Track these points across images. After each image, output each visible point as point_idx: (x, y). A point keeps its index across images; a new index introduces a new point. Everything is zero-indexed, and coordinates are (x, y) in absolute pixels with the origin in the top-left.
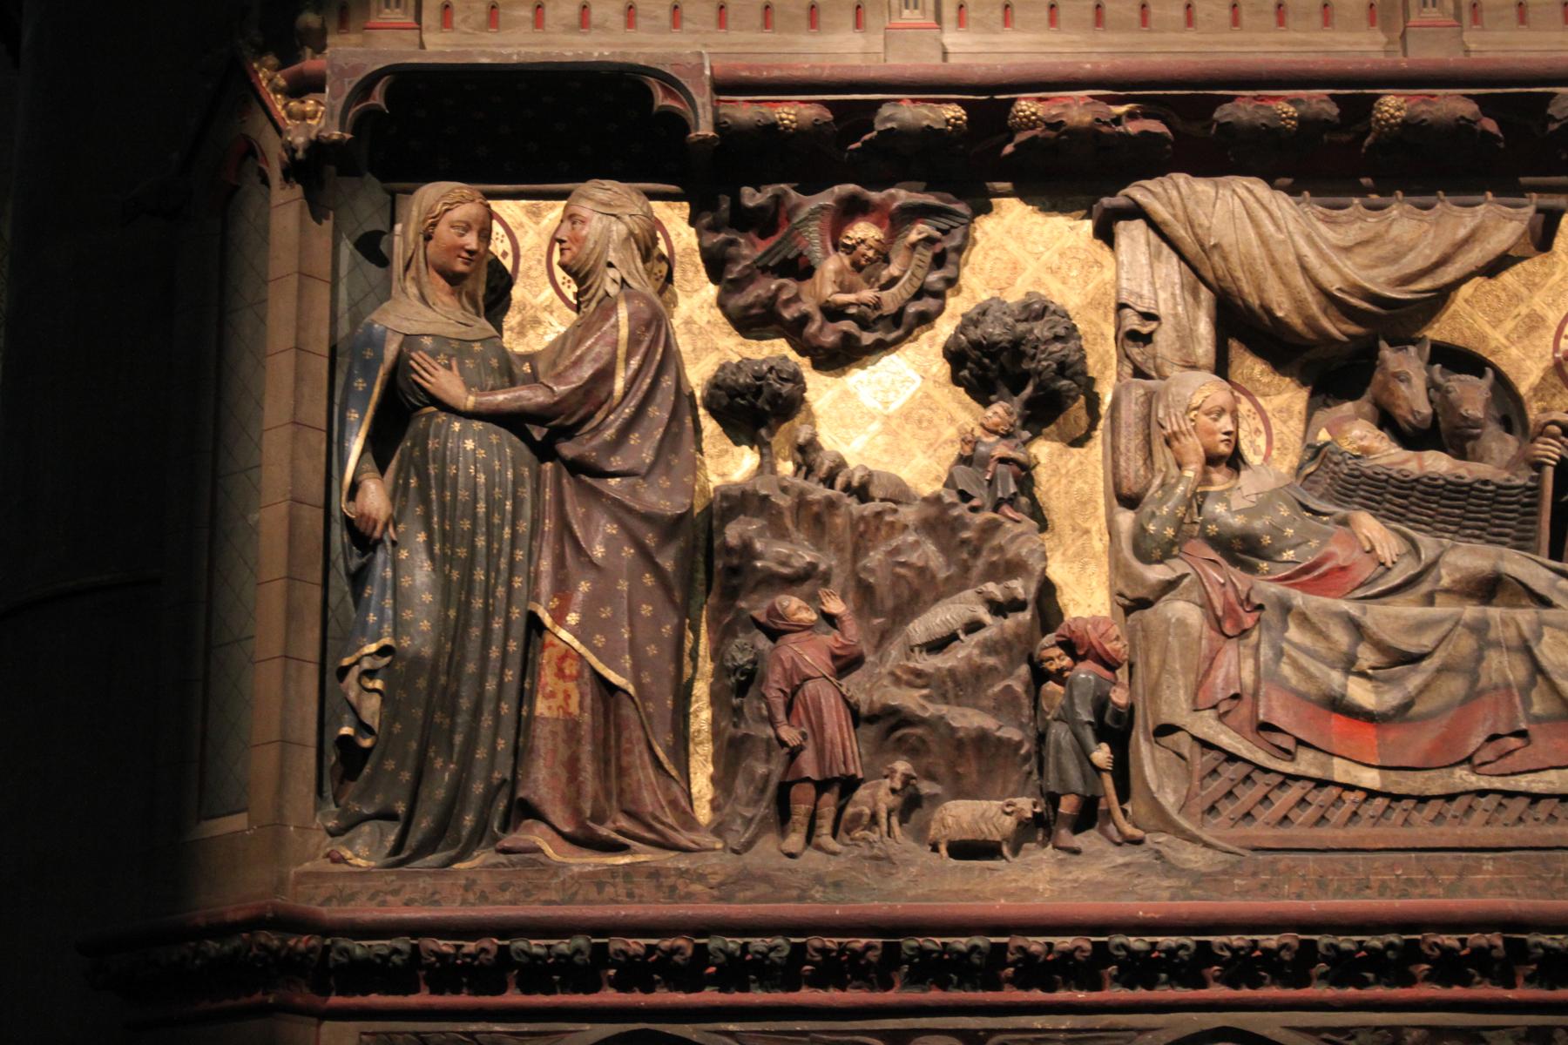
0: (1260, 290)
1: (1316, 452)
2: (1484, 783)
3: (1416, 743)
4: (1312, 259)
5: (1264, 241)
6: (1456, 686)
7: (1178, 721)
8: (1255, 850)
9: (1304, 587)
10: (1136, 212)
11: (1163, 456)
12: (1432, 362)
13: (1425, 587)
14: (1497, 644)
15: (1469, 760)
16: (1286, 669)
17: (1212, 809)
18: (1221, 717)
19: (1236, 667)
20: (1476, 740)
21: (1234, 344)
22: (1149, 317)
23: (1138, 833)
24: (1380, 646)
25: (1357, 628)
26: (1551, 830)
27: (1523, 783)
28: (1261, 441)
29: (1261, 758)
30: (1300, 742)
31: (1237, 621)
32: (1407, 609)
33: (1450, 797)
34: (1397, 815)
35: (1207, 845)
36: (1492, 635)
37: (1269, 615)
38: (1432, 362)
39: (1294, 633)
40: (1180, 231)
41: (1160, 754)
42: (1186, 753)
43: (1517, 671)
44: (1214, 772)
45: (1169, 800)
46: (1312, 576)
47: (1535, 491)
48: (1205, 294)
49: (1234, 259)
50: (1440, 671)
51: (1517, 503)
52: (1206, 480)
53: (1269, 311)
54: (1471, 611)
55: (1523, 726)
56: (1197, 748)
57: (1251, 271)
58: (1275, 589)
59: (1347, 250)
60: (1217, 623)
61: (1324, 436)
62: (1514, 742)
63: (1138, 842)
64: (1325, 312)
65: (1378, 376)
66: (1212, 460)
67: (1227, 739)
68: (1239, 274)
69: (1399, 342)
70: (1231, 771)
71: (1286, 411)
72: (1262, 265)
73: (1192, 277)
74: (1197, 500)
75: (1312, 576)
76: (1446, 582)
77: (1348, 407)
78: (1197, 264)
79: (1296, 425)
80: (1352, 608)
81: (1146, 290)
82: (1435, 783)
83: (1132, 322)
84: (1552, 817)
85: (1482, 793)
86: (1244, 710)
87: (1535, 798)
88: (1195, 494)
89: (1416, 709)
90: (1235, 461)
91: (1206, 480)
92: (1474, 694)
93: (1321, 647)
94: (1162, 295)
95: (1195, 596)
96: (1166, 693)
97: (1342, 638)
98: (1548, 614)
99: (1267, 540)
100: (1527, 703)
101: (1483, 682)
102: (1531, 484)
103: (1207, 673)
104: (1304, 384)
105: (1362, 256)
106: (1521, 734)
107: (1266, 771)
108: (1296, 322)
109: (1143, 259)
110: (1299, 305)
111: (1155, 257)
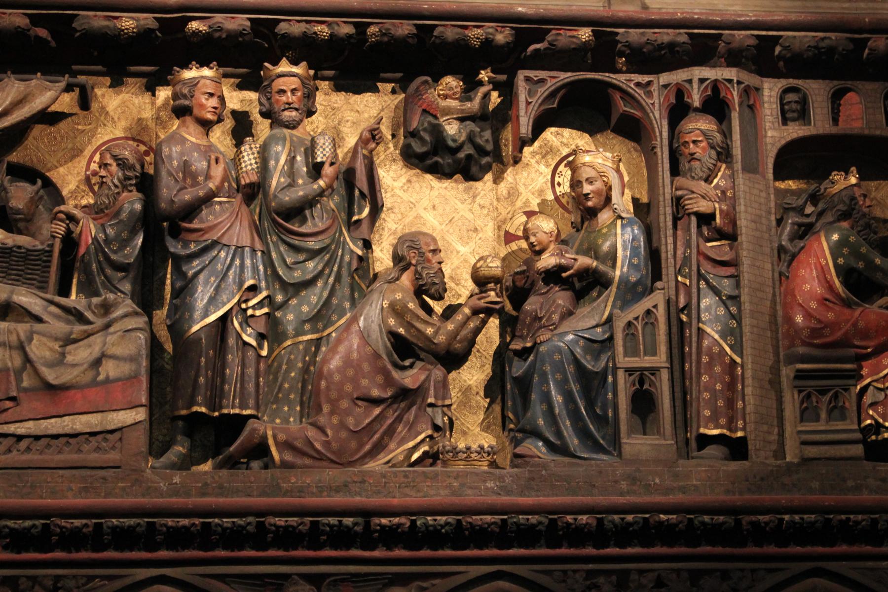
51: (40, 260)
98: (38, 327)
102: (47, 249)
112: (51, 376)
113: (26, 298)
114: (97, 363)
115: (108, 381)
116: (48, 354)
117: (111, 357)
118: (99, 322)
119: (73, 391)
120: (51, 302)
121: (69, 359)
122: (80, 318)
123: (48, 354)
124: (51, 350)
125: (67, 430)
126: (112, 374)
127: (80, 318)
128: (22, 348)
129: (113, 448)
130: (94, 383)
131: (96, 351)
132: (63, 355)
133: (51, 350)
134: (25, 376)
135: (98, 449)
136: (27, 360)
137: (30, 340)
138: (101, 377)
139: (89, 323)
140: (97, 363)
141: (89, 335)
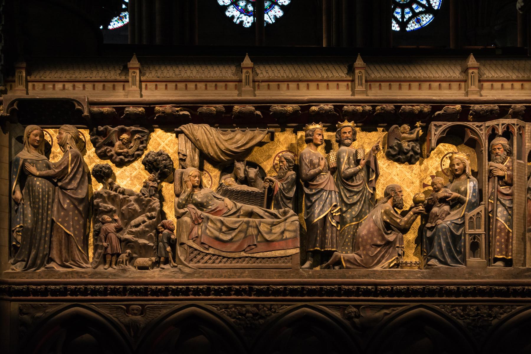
0: (207, 150)
1: (221, 185)
2: (247, 255)
3: (234, 247)
4: (218, 143)
5: (208, 139)
6: (242, 235)
7: (184, 242)
8: (200, 268)
9: (212, 214)
10: (182, 132)
11: (184, 186)
12: (246, 165)
13: (238, 214)
14: (251, 226)
15: (244, 250)
16: (207, 231)
17: (191, 260)
18: (194, 241)
19: (197, 231)
20: (245, 246)
21: (205, 161)
22: (184, 155)
23: (176, 265)
24: (227, 227)
25: (222, 222)
26: (260, 264)
27: (255, 255)
28: (210, 182)
29: (202, 250)
30: (210, 247)
31: (198, 221)
32: (233, 219)
33: (240, 258)
34: (229, 262)
35: (190, 267)
36: (250, 224)
37: (205, 220)
38: (246, 165)
39: (210, 224)
40: (191, 137)
41: (182, 249)
42: (186, 248)
43: (255, 232)
44: (192, 253)
45: (182, 258)
46: (215, 212)
47: (264, 194)
48: (197, 150)
49: (202, 143)
50: (240, 232)
52: (193, 191)
53: (209, 154)
54: (246, 219)
55: (256, 243)
56: (189, 248)
57: (205, 144)
58: (206, 214)
59: (226, 141)
60: (193, 222)
61: (223, 181)
62: (253, 247)
63: (176, 267)
64: (222, 154)
65: (235, 168)
66: (194, 187)
67: (195, 246)
68: (203, 146)
69: (239, 161)
70: (195, 252)
71: (215, 176)
72: (208, 144)
73: (194, 146)
74: (191, 195)
75: (215, 212)
76: (242, 213)
77: (229, 175)
78: (195, 144)
79: (218, 179)
80: (222, 218)
81: (184, 150)
82: (237, 255)
83: (181, 157)
84: (261, 262)
85: (247, 257)
86: (199, 240)
87: (258, 258)
88: (190, 193)
89: (234, 240)
90: (201, 186)
91: (193, 191)
92: (245, 237)
93: (215, 227)
94: (188, 151)
95: (189, 216)
96: (182, 236)
97: (219, 225)
99: (205, 204)
100: (257, 239)
101: (248, 234)
103: (191, 232)
104: (220, 170)
105: (230, 142)
106: (255, 245)
107: (203, 252)
108: (215, 157)
109: (184, 142)
110: (216, 153)
111: (186, 142)
112: (267, 237)
113: (257, 209)
114: (283, 233)
115: (286, 239)
116: (266, 229)
117: (288, 231)
118: (283, 218)
119: (275, 243)
120: (266, 211)
121: (273, 231)
122: (276, 217)
123: (266, 229)
124: (267, 228)
125: (273, 256)
126: (288, 237)
127: (276, 217)
128: (257, 227)
129: (289, 262)
130: (282, 240)
131: (282, 228)
132: (271, 230)
133: (267, 228)
134: (259, 237)
135: (284, 262)
136: (259, 232)
137: (260, 225)
138: (284, 238)
139: (279, 218)
140: (283, 233)
141: (279, 223)
